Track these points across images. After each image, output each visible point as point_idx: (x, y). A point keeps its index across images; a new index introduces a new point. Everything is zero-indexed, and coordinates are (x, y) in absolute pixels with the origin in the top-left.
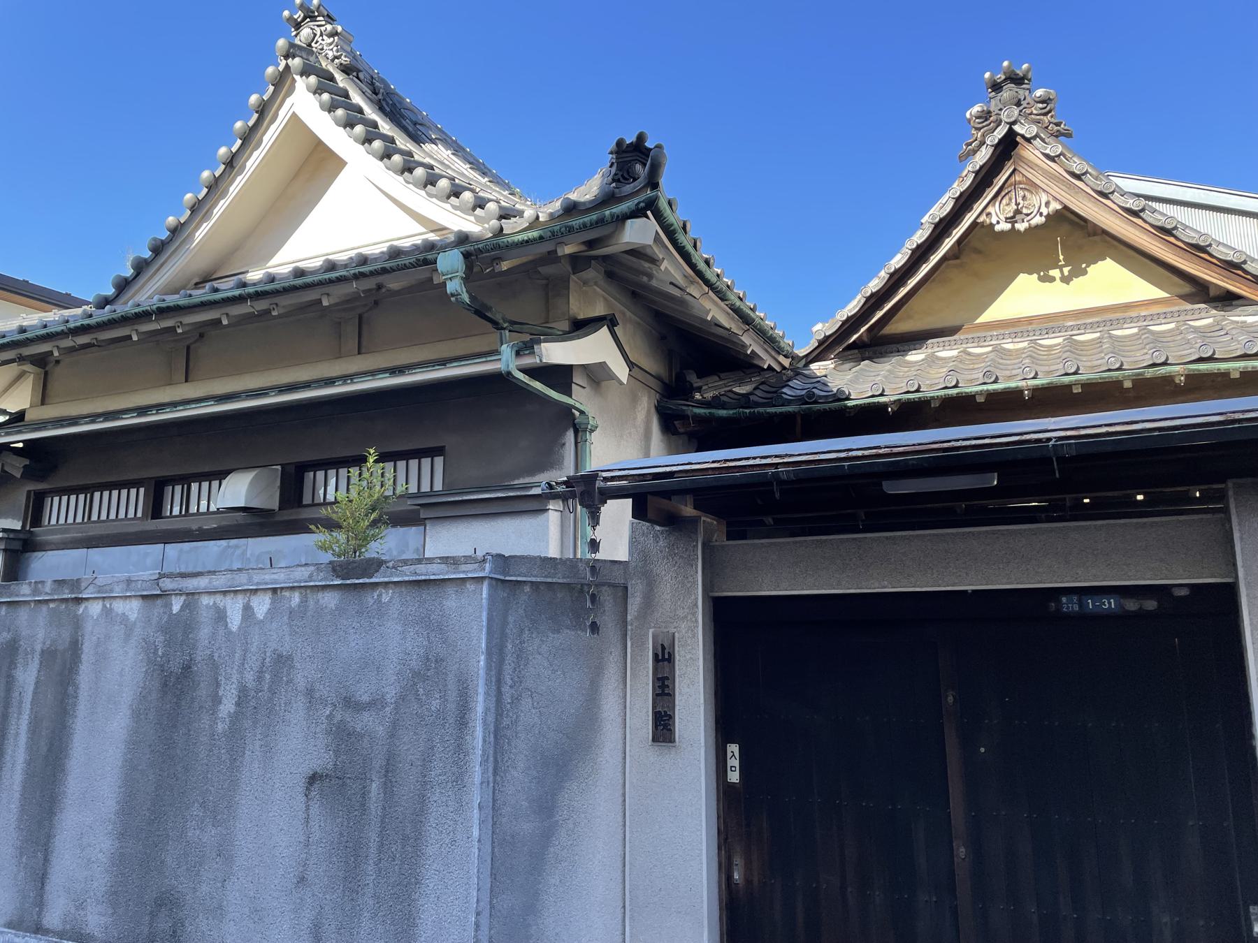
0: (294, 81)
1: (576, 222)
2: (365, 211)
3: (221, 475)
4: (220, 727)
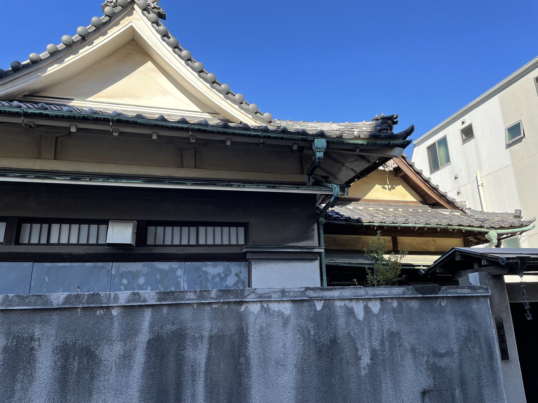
0: (133, 9)
1: (379, 142)
2: (161, 90)
3: (106, 222)
4: (363, 373)
